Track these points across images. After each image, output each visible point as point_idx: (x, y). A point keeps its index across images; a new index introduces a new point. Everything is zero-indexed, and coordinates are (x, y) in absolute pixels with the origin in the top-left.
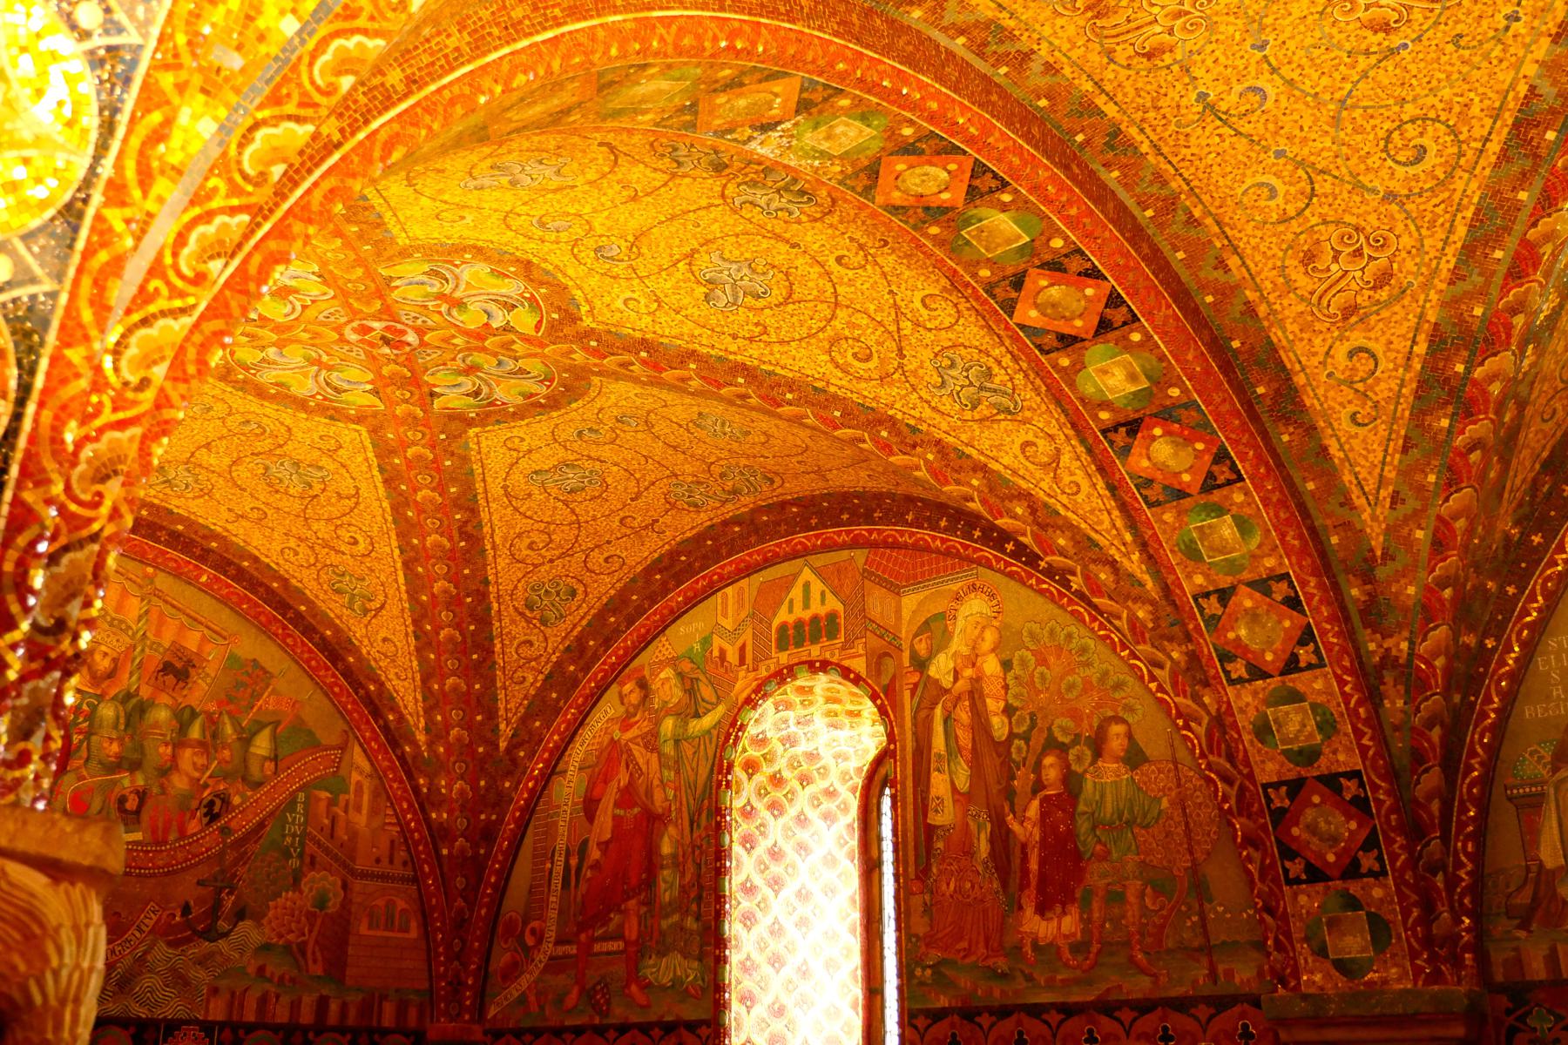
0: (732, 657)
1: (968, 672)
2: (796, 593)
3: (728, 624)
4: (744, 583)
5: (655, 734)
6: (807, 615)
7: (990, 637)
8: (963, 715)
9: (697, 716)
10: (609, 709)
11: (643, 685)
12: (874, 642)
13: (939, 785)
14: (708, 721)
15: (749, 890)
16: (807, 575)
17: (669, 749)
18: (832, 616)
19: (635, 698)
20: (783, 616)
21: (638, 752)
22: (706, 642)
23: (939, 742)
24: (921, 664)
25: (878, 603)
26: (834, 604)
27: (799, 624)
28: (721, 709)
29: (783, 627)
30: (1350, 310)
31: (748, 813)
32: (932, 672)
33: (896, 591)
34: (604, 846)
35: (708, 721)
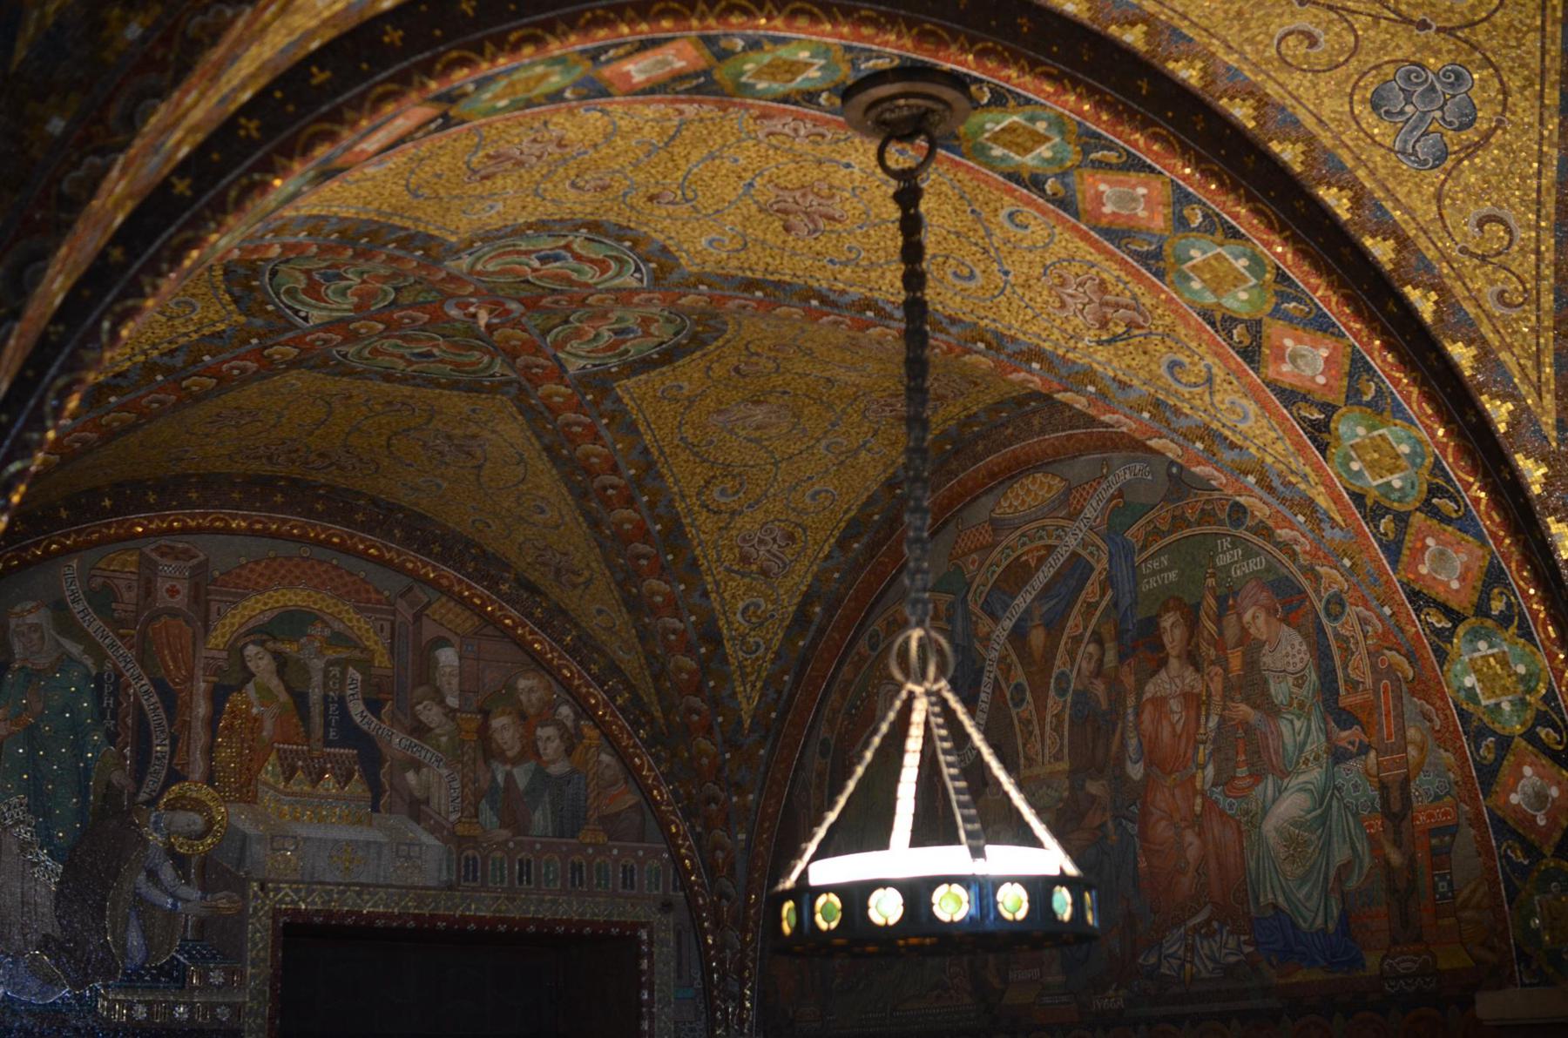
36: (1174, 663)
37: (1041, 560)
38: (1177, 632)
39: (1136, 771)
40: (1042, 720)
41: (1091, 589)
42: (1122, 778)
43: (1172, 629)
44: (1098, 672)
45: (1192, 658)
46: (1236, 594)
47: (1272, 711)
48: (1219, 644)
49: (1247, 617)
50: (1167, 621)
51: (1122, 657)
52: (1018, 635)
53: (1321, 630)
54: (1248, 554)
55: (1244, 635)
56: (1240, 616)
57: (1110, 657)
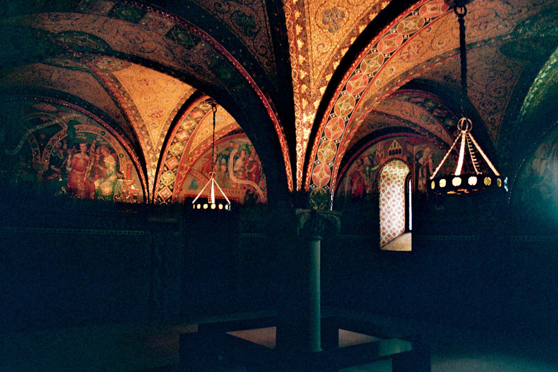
0: (380, 155)
1: (426, 162)
2: (393, 144)
3: (379, 149)
4: (383, 141)
5: (365, 170)
6: (395, 149)
7: (430, 156)
8: (425, 170)
9: (373, 167)
10: (354, 165)
11: (362, 160)
12: (408, 155)
13: (420, 183)
14: (375, 168)
15: (384, 200)
16: (395, 141)
17: (368, 173)
18: (400, 150)
19: (360, 162)
20: (390, 149)
21: (361, 173)
22: (375, 153)
23: (420, 175)
24: (417, 160)
25: (409, 147)
26: (400, 147)
27: (393, 151)
28: (378, 166)
29: (390, 151)
30: (490, 112)
31: (383, 186)
32: (419, 161)
33: (413, 145)
34: (355, 191)
35: (375, 168)
36: (82, 153)
37: (46, 121)
38: (84, 148)
39: (69, 169)
40: (42, 154)
41: (62, 132)
42: (64, 170)
43: (83, 146)
44: (61, 148)
45: (88, 154)
46: (100, 146)
47: (106, 168)
48: (95, 152)
49: (102, 151)
50: (82, 145)
51: (68, 147)
52: (37, 134)
53: (118, 158)
54: (104, 140)
55: (101, 153)
56: (100, 151)
57: (65, 147)
